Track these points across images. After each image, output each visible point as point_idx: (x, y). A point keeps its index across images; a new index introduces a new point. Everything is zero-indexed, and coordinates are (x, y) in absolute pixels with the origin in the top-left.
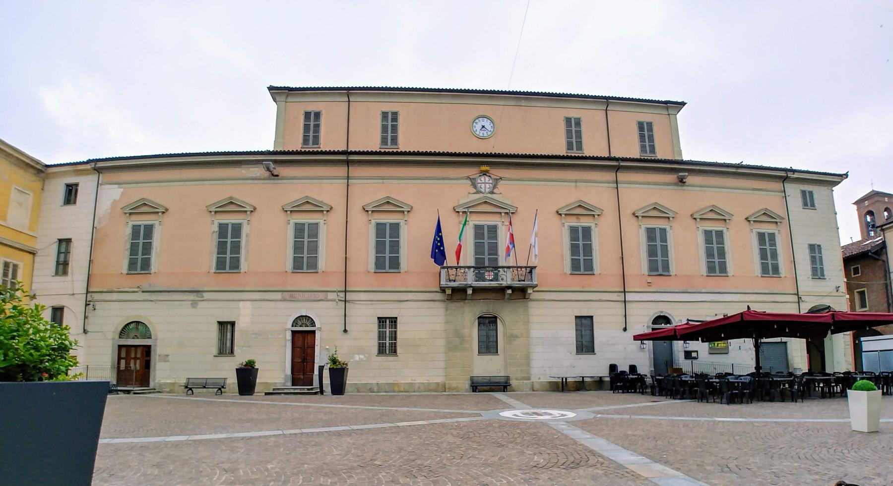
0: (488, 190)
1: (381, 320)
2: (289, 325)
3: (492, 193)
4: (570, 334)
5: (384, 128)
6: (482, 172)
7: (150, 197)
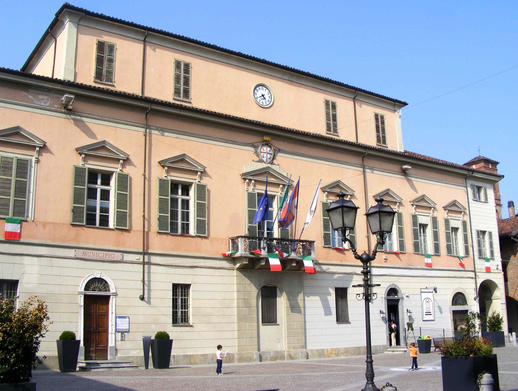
0: (269, 161)
1: (175, 286)
2: (82, 290)
3: (272, 163)
4: (437, 290)
5: (177, 79)
6: (264, 141)
7: (110, 140)
